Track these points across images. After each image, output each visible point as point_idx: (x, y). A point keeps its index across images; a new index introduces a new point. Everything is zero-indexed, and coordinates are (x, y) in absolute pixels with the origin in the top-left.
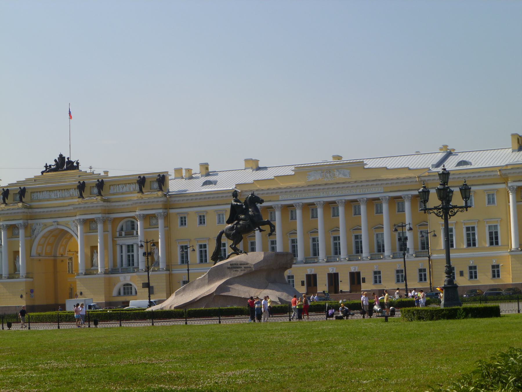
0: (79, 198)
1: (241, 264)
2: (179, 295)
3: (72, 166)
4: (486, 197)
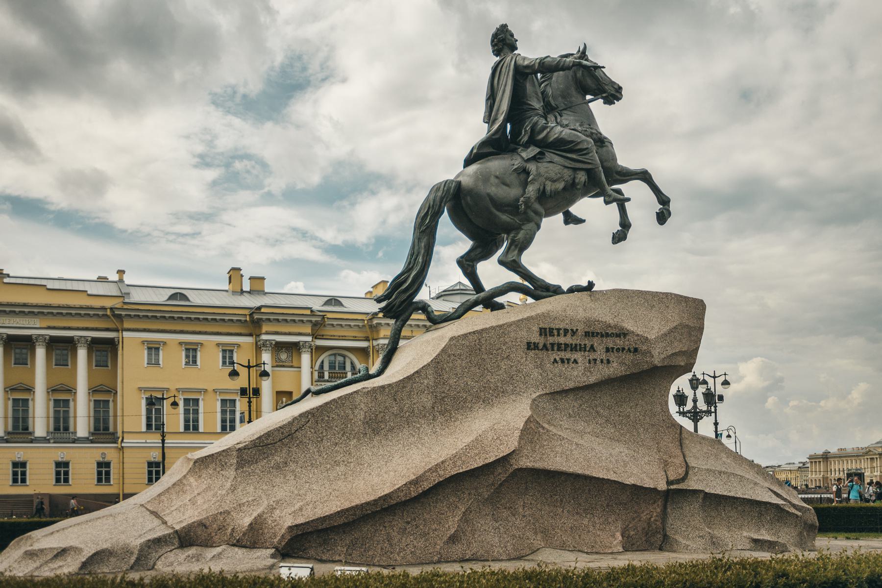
1: (587, 334)
2: (258, 467)
4: (221, 354)
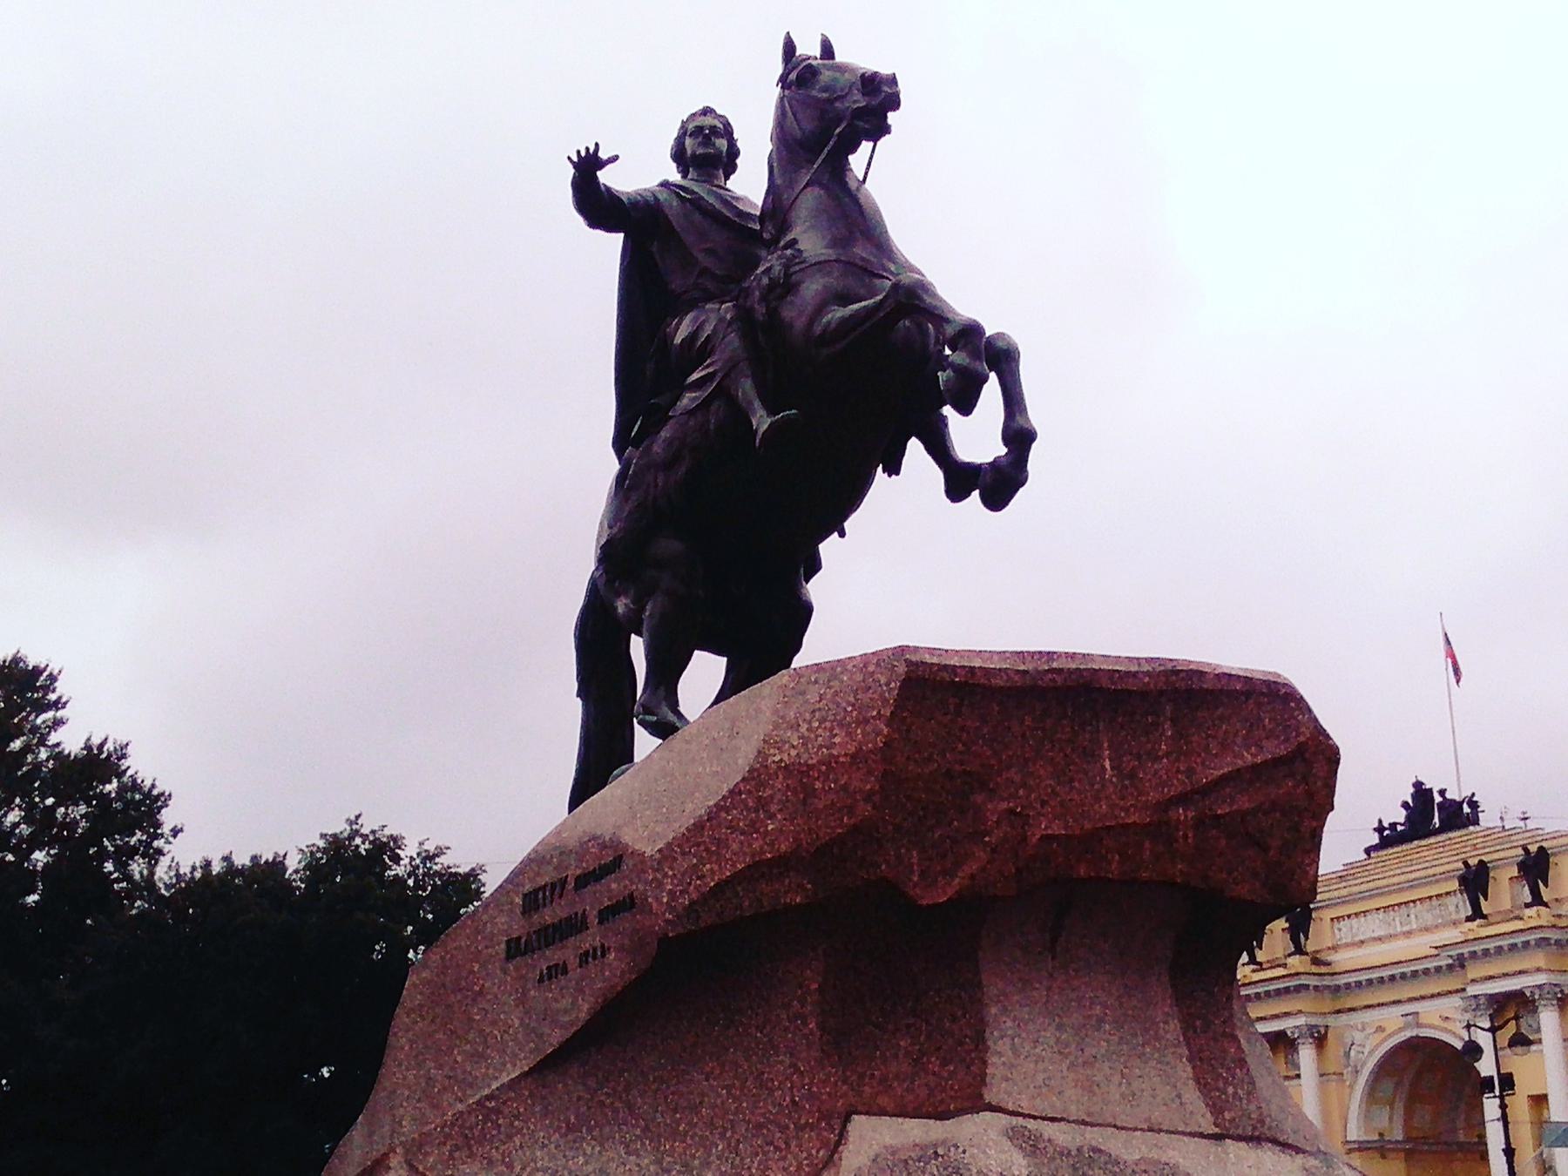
0: (1469, 919)
1: (583, 881)
3: (1459, 815)
